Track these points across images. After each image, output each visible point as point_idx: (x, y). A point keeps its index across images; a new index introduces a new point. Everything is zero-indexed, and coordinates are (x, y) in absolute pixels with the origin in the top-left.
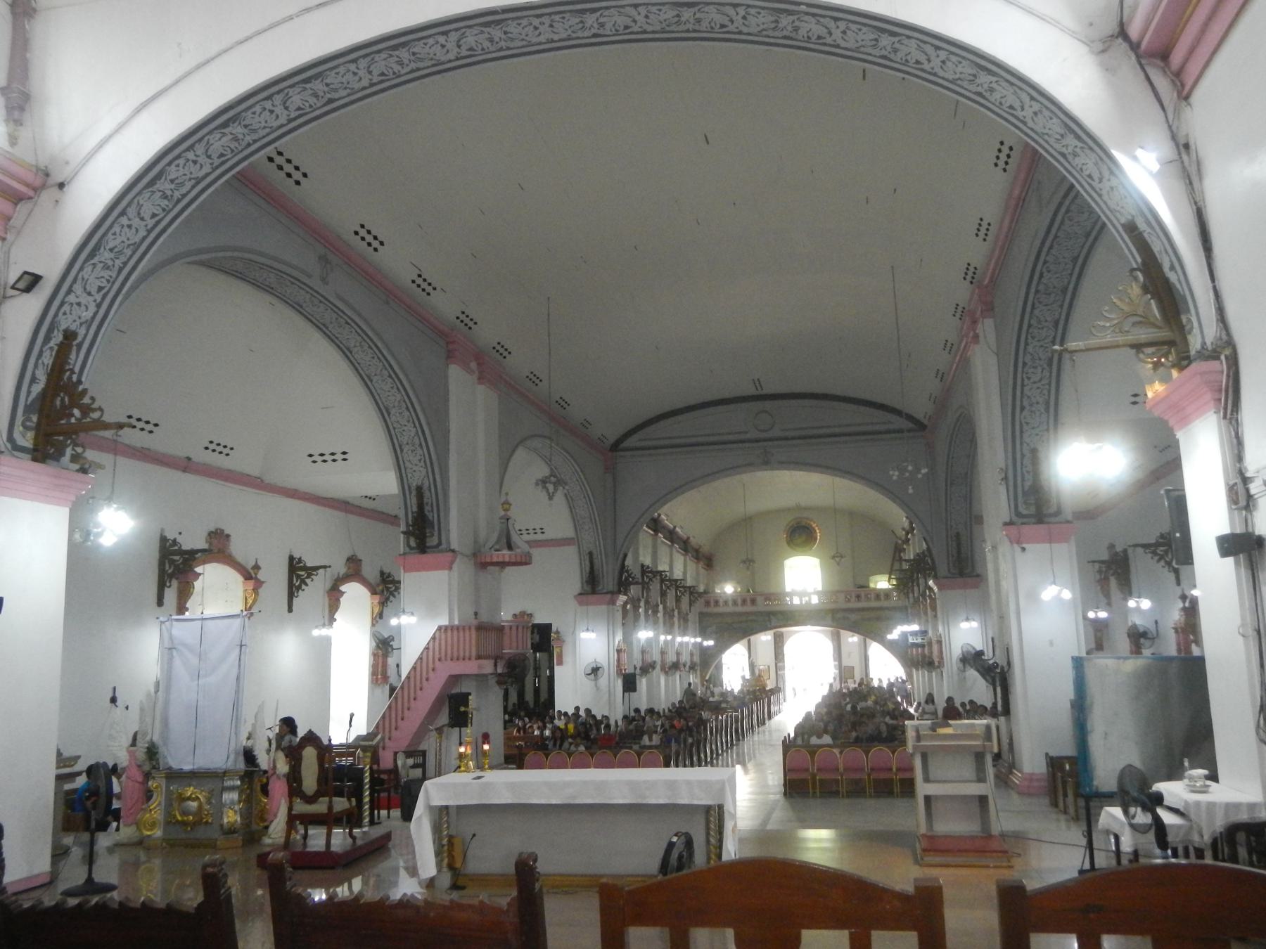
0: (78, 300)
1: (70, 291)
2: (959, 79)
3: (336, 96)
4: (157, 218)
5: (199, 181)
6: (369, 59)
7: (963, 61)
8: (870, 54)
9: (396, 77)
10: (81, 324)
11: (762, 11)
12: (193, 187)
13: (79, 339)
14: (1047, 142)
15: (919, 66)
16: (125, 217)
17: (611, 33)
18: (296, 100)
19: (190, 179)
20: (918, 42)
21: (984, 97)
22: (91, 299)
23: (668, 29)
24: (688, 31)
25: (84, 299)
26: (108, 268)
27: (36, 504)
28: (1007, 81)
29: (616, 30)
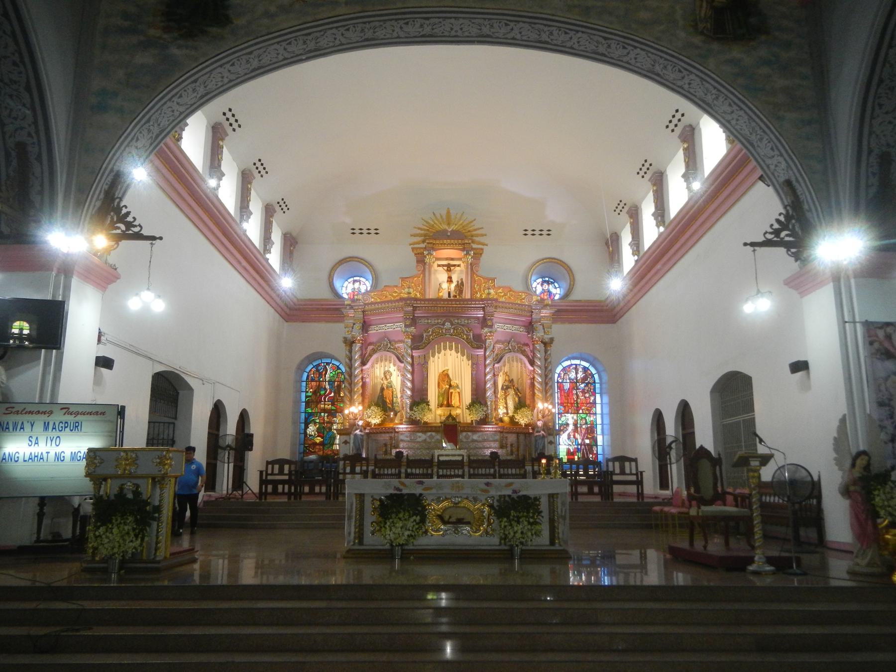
1: (768, 167)
3: (601, 39)
4: (732, 104)
5: (702, 79)
6: (564, 44)
7: (216, 87)
9: (561, 27)
11: (326, 46)
13: (793, 179)
17: (418, 20)
18: (620, 52)
19: (703, 84)
20: (240, 75)
21: (192, 82)
22: (776, 157)
23: (381, 23)
24: (369, 22)
27: (817, 291)
28: (195, 103)
29: (414, 21)
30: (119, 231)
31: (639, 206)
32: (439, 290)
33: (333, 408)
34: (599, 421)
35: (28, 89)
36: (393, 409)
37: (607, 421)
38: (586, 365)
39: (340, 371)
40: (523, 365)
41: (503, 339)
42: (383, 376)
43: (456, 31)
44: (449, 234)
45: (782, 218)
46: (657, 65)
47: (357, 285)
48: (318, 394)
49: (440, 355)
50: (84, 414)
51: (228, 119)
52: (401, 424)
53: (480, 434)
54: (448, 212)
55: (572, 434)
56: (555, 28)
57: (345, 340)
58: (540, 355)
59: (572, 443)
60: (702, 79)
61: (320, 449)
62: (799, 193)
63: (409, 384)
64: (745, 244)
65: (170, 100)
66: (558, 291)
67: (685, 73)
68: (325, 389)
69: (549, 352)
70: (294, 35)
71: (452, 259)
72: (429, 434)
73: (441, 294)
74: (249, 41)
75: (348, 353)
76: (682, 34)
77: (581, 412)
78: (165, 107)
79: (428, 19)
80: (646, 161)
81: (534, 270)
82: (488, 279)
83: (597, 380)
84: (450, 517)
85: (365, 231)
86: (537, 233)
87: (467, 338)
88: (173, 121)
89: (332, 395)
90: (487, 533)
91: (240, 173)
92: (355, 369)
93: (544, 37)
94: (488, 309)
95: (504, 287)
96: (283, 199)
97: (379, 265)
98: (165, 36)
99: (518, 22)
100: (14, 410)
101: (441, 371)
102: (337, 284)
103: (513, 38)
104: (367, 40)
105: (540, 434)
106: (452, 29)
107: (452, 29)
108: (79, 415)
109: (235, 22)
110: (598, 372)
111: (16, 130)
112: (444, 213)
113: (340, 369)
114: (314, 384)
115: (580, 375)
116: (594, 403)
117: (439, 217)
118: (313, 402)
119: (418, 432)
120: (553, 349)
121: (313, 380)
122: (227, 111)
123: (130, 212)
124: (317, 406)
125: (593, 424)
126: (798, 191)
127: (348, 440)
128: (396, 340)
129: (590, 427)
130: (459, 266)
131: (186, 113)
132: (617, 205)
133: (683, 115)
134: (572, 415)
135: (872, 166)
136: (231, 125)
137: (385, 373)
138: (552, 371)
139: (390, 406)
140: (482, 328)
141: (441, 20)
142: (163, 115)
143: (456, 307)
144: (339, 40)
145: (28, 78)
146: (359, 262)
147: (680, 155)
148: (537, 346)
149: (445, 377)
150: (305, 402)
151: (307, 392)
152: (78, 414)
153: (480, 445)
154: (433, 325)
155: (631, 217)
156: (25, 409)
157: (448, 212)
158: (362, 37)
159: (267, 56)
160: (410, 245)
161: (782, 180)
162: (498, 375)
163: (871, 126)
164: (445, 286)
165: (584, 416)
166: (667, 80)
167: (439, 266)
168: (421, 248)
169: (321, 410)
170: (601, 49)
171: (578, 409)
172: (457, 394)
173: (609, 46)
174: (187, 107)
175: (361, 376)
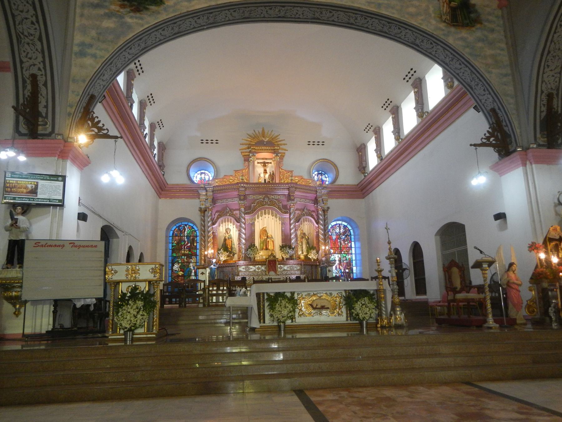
0: (484, 100)
1: (480, 101)
2: (149, 37)
3: (386, 23)
6: (363, 25)
7: (151, 44)
10: (493, 103)
11: (220, 21)
12: (448, 51)
13: (496, 108)
16: (460, 74)
18: (397, 31)
19: (444, 52)
22: (486, 95)
24: (249, 7)
25: (485, 97)
26: (478, 85)
27: (511, 172)
28: (138, 53)
29: (275, 8)
30: (93, 133)
31: (380, 127)
32: (259, 178)
33: (190, 253)
34: (354, 258)
35: (40, 39)
36: (231, 252)
37: (359, 257)
38: (346, 224)
39: (194, 230)
40: (312, 224)
41: (300, 207)
42: (224, 231)
43: (300, 15)
44: (265, 143)
45: (490, 130)
46: (418, 40)
47: (203, 176)
48: (180, 244)
49: (262, 218)
50: (84, 247)
51: (137, 67)
52: (240, 261)
53: (289, 266)
54: (263, 130)
55: (338, 266)
56: (359, 15)
57: (200, 210)
58: (322, 217)
59: (338, 272)
60: (444, 48)
61: (182, 279)
62: (500, 116)
63: (244, 236)
64: (471, 145)
65: (125, 50)
66: (328, 179)
67: (434, 44)
68: (185, 241)
69: (326, 216)
70: (203, 13)
71: (266, 159)
72: (257, 266)
73: (260, 180)
75: (203, 218)
76: (434, 22)
77: (343, 253)
79: (284, 7)
80: (388, 100)
81: (314, 166)
82: (289, 172)
83: (352, 234)
84: (317, 305)
85: (210, 142)
86: (316, 143)
87: (279, 207)
89: (189, 245)
90: (339, 314)
91: (139, 103)
92: (209, 227)
93: (352, 21)
94: (291, 189)
95: (298, 177)
96: (161, 120)
97: (219, 163)
98: (122, 10)
99: (338, 11)
100: (40, 244)
101: (261, 228)
102: (192, 174)
103: (333, 21)
105: (325, 265)
106: (297, 13)
107: (297, 13)
108: (81, 248)
109: (167, 4)
110: (353, 229)
111: (31, 66)
112: (261, 131)
113: (194, 228)
114: (177, 238)
115: (342, 230)
116: (351, 247)
117: (257, 132)
118: (177, 249)
119: (250, 265)
120: (329, 213)
121: (176, 236)
123: (100, 121)
124: (179, 252)
125: (350, 260)
126: (499, 115)
127: (205, 272)
128: (234, 209)
129: (349, 262)
130: (271, 163)
131: (132, 59)
132: (366, 127)
133: (415, 72)
134: (338, 255)
135: (543, 101)
136: (138, 71)
137: (226, 230)
138: (328, 227)
139: (230, 250)
140: (288, 201)
141: (292, 8)
143: (271, 188)
144: (229, 18)
146: (206, 161)
147: (412, 95)
148: (320, 212)
149: (264, 231)
150: (172, 250)
151: (173, 243)
152: (80, 247)
153: (289, 272)
154: (257, 199)
155: (376, 134)
156: (47, 243)
157: (263, 130)
160: (240, 150)
161: (489, 108)
162: (298, 230)
163: (543, 77)
164: (262, 175)
165: (345, 255)
166: (422, 49)
167: (258, 163)
168: (246, 152)
169: (182, 254)
170: (385, 29)
171: (341, 251)
172: (272, 242)
173: (390, 28)
174: (134, 55)
175: (212, 232)
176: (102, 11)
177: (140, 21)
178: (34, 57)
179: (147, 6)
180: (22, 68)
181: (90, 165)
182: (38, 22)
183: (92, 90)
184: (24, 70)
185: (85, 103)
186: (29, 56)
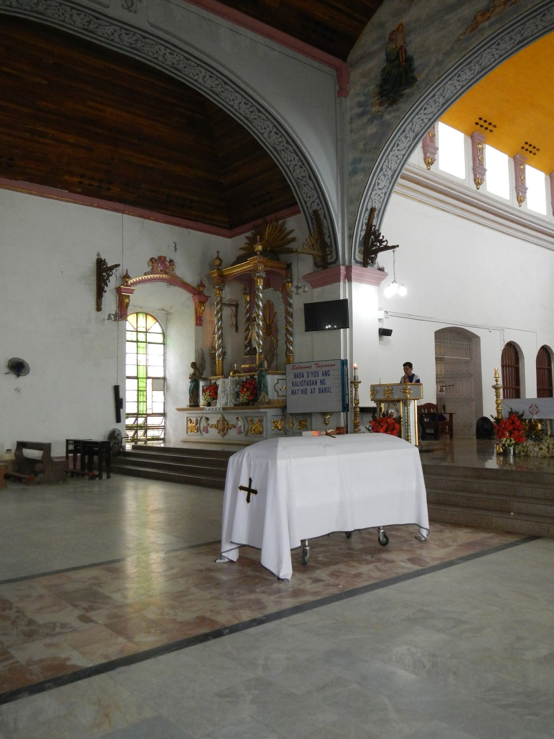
2: (413, 124)
8: (438, 90)
14: (385, 161)
15: (423, 108)
20: (435, 113)
35: (310, 178)
65: (391, 150)
74: (428, 89)
78: (390, 156)
88: (400, 162)
98: (381, 109)
104: (520, 42)
109: (419, 79)
111: (312, 204)
122: (478, 121)
142: (390, 161)
145: (309, 173)
158: (514, 43)
159: (447, 91)
174: (408, 148)
176: (365, 119)
177: (397, 113)
178: (312, 195)
179: (402, 92)
180: (307, 208)
181: (387, 277)
182: (303, 164)
183: (370, 204)
184: (309, 209)
185: (366, 219)
186: (308, 196)
